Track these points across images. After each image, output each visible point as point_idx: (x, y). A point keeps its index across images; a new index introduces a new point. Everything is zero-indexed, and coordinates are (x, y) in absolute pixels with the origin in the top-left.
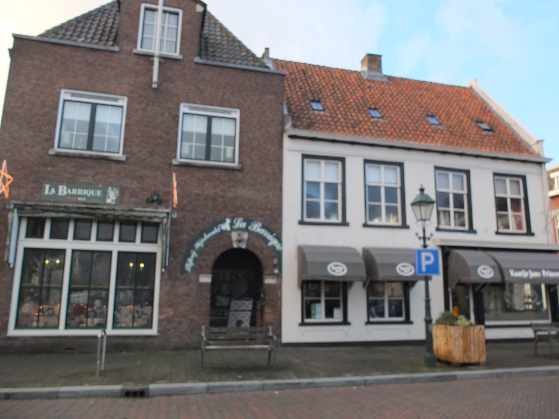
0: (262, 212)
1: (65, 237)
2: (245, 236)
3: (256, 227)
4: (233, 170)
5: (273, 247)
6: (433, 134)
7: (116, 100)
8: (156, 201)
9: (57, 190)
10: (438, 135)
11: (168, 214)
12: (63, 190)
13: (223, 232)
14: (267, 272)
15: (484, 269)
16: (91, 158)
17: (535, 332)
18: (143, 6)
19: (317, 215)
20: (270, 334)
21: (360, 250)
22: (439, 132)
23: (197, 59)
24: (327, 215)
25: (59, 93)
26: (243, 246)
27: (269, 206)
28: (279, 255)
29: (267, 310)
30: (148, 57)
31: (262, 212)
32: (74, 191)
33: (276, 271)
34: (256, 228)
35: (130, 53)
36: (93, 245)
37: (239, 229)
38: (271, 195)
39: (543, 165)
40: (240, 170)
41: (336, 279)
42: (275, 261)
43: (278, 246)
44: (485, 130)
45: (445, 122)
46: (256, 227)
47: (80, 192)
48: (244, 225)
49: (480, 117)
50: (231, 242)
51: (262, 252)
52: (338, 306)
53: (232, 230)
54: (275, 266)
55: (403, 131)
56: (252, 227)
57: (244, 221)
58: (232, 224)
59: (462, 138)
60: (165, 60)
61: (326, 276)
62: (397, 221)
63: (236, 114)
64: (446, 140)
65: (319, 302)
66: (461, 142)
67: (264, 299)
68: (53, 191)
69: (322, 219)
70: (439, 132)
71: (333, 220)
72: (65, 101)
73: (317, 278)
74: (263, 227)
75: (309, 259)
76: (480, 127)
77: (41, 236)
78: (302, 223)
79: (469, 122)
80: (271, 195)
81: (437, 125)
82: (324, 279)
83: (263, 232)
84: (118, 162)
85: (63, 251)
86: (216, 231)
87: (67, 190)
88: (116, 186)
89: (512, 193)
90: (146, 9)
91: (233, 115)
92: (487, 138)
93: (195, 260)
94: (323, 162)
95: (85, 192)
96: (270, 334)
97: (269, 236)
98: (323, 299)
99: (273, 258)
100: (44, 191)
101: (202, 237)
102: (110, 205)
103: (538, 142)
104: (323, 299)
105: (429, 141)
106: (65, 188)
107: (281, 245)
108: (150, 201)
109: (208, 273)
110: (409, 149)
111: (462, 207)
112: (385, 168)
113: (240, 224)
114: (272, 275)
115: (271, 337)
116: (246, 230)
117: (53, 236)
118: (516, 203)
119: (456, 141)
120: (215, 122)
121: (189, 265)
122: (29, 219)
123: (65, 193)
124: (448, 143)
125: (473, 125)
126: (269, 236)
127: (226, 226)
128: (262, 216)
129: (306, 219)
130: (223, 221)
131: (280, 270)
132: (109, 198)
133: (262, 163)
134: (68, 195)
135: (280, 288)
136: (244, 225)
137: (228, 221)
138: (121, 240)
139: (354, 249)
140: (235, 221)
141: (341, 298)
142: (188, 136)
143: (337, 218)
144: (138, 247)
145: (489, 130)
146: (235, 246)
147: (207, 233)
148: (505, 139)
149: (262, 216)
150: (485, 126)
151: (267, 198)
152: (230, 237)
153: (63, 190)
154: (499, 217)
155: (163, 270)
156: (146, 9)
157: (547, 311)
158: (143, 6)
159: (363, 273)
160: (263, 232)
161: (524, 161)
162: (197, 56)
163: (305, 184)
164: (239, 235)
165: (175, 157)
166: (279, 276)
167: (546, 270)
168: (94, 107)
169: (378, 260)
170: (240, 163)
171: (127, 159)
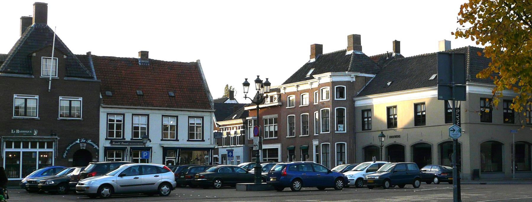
1: (20, 147)
2: (85, 145)
4: (79, 120)
5: (96, 148)
7: (34, 97)
8: (54, 135)
9: (16, 131)
11: (57, 138)
12: (18, 131)
16: (27, 119)
18: (42, 57)
23: (65, 78)
25: (13, 96)
26: (85, 148)
28: (98, 151)
30: (46, 80)
32: (22, 132)
36: (29, 150)
37: (83, 142)
46: (89, 141)
47: (24, 132)
50: (80, 147)
54: (97, 155)
57: (84, 140)
58: (80, 141)
63: (81, 99)
68: (14, 132)
84: (37, 120)
86: (74, 143)
87: (19, 131)
88: (37, 129)
90: (43, 58)
91: (80, 99)
93: (67, 154)
95: (26, 132)
97: (94, 145)
100: (11, 132)
101: (69, 146)
102: (35, 136)
106: (19, 130)
107: (99, 148)
109: (72, 158)
112: (141, 116)
113: (83, 141)
116: (85, 142)
121: (64, 156)
123: (19, 132)
126: (94, 145)
127: (78, 142)
130: (77, 140)
131: (98, 156)
132: (35, 133)
134: (20, 133)
137: (79, 140)
138: (40, 148)
140: (81, 140)
142: (62, 108)
144: (46, 150)
146: (81, 148)
147: (71, 145)
152: (80, 146)
153: (18, 131)
155: (55, 158)
156: (43, 58)
157: (188, 170)
158: (42, 57)
162: (65, 77)
164: (83, 144)
165: (58, 117)
168: (26, 100)
170: (82, 118)
171: (40, 119)
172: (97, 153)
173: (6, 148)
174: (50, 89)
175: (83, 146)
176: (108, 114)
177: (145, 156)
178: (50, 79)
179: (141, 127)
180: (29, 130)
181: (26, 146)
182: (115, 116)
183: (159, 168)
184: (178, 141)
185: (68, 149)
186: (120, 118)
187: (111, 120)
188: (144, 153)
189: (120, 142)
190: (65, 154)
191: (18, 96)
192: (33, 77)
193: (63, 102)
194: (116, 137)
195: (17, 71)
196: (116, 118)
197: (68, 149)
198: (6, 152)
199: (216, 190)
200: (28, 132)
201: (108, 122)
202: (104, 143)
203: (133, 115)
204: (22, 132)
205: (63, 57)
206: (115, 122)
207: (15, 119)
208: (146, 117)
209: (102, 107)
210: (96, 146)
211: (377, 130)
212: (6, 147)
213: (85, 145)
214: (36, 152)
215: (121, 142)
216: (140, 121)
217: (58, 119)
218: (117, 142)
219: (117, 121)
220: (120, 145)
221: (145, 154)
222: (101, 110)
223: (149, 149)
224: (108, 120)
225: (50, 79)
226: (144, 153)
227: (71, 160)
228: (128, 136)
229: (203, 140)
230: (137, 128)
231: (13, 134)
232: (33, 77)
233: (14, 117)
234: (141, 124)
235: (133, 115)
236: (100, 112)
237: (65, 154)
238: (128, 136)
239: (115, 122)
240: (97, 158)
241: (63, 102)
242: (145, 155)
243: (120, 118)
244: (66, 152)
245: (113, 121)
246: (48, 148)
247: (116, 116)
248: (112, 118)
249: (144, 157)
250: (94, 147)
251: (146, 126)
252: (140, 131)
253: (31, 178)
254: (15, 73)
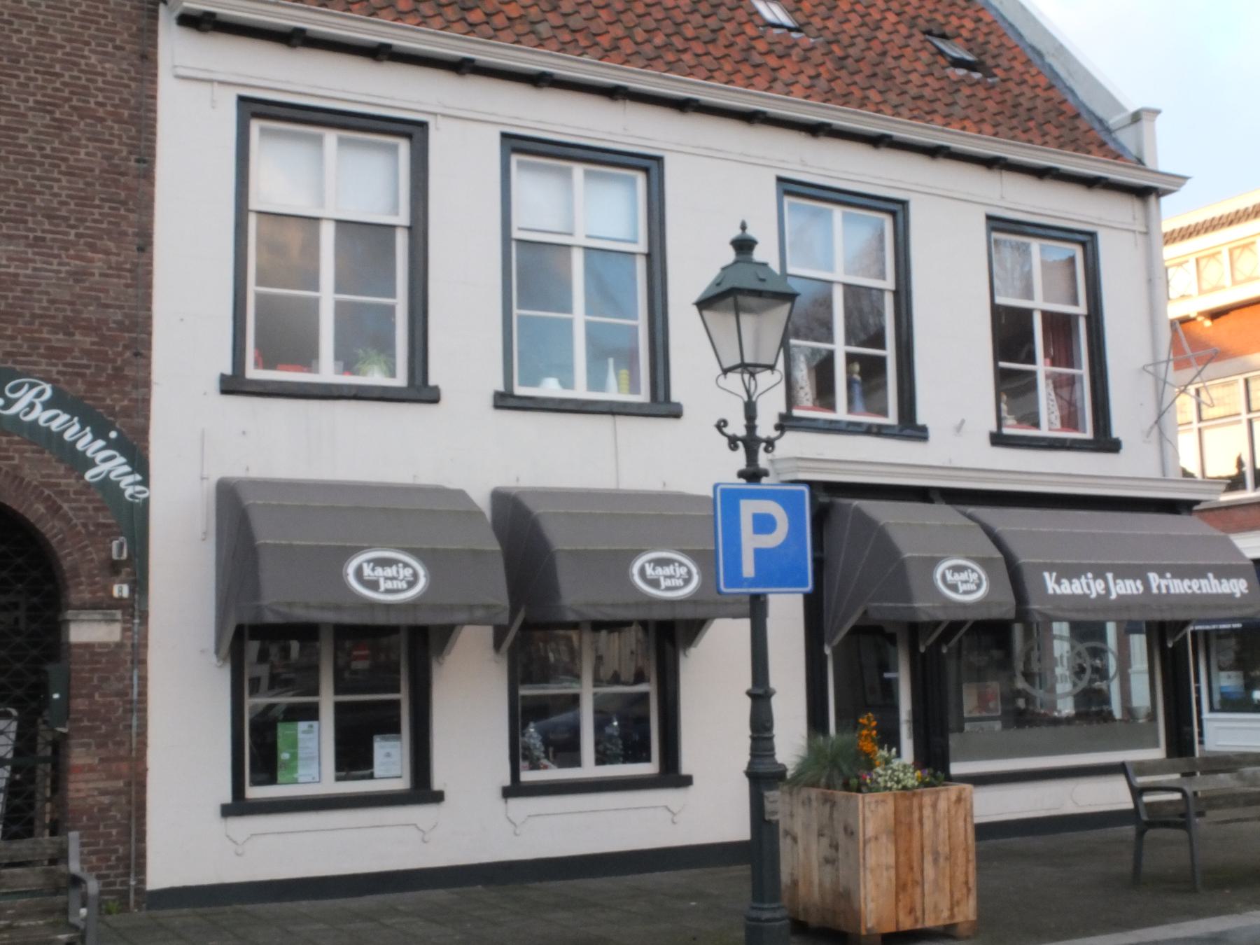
0: (58, 339)
5: (108, 486)
6: (773, 61)
10: (790, 66)
14: (79, 593)
15: (958, 569)
17: (1137, 792)
19: (308, 358)
20: (75, 866)
21: (481, 499)
22: (796, 54)
24: (347, 361)
27: (91, 312)
29: (79, 756)
31: (58, 339)
33: (121, 590)
34: (31, 406)
38: (98, 263)
39: (1152, 199)
41: (381, 619)
42: (118, 549)
43: (129, 485)
44: (958, 63)
45: (817, 22)
49: (940, 18)
51: (55, 510)
52: (392, 728)
54: (114, 568)
55: (659, 40)
56: (9, 403)
59: (879, 84)
61: (338, 608)
62: (634, 388)
64: (822, 83)
65: (311, 713)
66: (873, 95)
67: (65, 712)
69: (327, 372)
70: (796, 54)
71: (375, 377)
73: (301, 614)
75: (265, 535)
76: (941, 53)
78: (233, 385)
79: (903, 29)
80: (98, 263)
81: (790, 29)
82: (331, 617)
83: (59, 421)
89: (1046, 299)
92: (966, 91)
94: (331, 137)
96: (75, 866)
97: (88, 444)
98: (327, 701)
99: (109, 532)
103: (1136, 117)
104: (327, 701)
105: (761, 81)
107: (145, 482)
110: (683, 106)
111: (878, 341)
114: (104, 606)
115: (76, 881)
118: (1059, 326)
119: (858, 93)
124: (829, 96)
125: (915, 43)
126: (88, 444)
128: (54, 353)
129: (253, 372)
131: (140, 584)
133: (60, 126)
135: (140, 661)
139: (461, 495)
141: (403, 696)
143: (392, 374)
145: (970, 66)
148: (1026, 104)
149: (54, 353)
150: (956, 50)
151: (78, 276)
154: (1003, 379)
159: (496, 591)
160: (59, 421)
161: (1091, 183)
163: (252, 221)
167: (1161, 573)
169: (560, 538)
177: (759, 553)
184: (921, 434)
203: (514, 144)
208: (633, 181)
210: (112, 466)
229: (1105, 442)
240: (119, 604)
249: (748, 570)
250: (88, 475)
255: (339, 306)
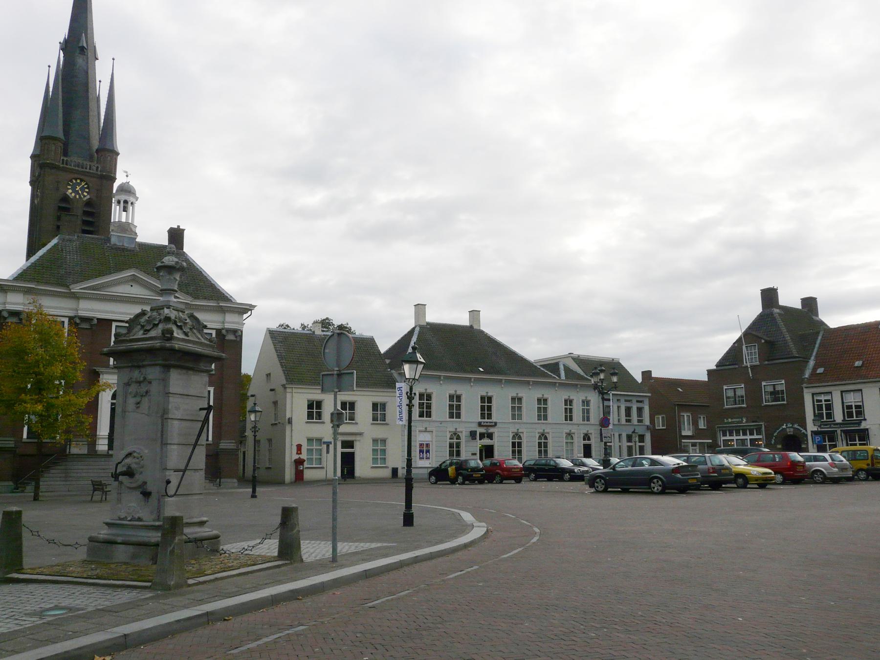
2: (792, 430)
3: (796, 426)
12: (730, 420)
13: (783, 429)
26: (792, 434)
28: (806, 436)
32: (733, 420)
35: (742, 367)
40: (787, 404)
43: (805, 432)
46: (796, 426)
47: (735, 420)
48: (791, 425)
50: (787, 433)
53: (787, 428)
58: (786, 425)
60: (753, 367)
72: (726, 389)
74: (799, 425)
77: (726, 436)
83: (799, 427)
85: (733, 440)
97: (801, 429)
108: (753, 422)
113: (790, 425)
116: (791, 427)
117: (730, 436)
120: (776, 386)
122: (722, 431)
126: (801, 429)
127: (784, 427)
130: (783, 425)
131: (807, 442)
136: (791, 425)
137: (785, 425)
138: (750, 435)
146: (789, 434)
153: (730, 420)
160: (799, 427)
163: (816, 406)
165: (763, 403)
166: (807, 444)
172: (805, 439)
173: (723, 436)
174: (751, 376)
175: (790, 431)
176: (813, 395)
178: (749, 366)
179: (855, 406)
180: (739, 418)
181: (738, 434)
182: (823, 395)
183: (818, 457)
185: (775, 435)
186: (828, 397)
187: (818, 401)
188: (816, 438)
189: (829, 424)
190: (773, 440)
191: (727, 387)
192: (737, 366)
193: (767, 386)
194: (827, 419)
195: (728, 364)
196: (823, 398)
197: (775, 435)
198: (723, 440)
199: (564, 482)
200: (738, 420)
201: (816, 403)
202: (811, 427)
204: (733, 420)
205: (761, 341)
206: (823, 403)
207: (726, 409)
209: (806, 387)
210: (804, 431)
211: (183, 446)
212: (723, 436)
213: (792, 430)
214: (747, 439)
215: (830, 424)
216: (852, 399)
217: (763, 405)
218: (826, 425)
219: (826, 401)
220: (830, 428)
221: (818, 439)
222: (805, 390)
223: (866, 431)
224: (815, 400)
225: (749, 366)
226: (816, 438)
227: (779, 446)
228: (838, 417)
230: (850, 407)
231: (726, 423)
232: (737, 366)
233: (726, 406)
234: (855, 402)
235: (842, 392)
236: (805, 394)
237: (773, 440)
238: (838, 417)
239: (823, 403)
241: (767, 386)
242: (819, 440)
243: (828, 397)
244: (774, 438)
245: (821, 401)
246: (730, 436)
247: (824, 396)
248: (819, 398)
251: (861, 404)
252: (854, 410)
253: (754, 464)
254: (726, 365)
255: (826, 413)
